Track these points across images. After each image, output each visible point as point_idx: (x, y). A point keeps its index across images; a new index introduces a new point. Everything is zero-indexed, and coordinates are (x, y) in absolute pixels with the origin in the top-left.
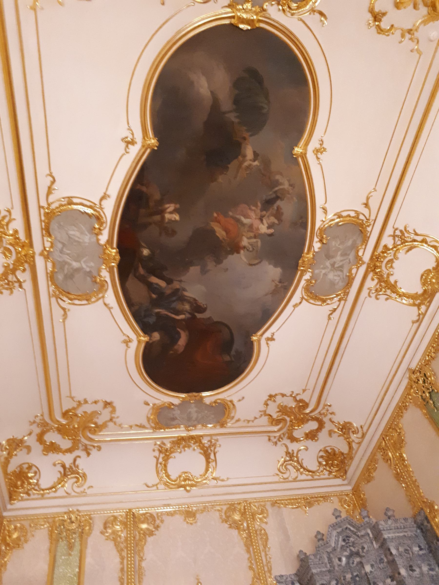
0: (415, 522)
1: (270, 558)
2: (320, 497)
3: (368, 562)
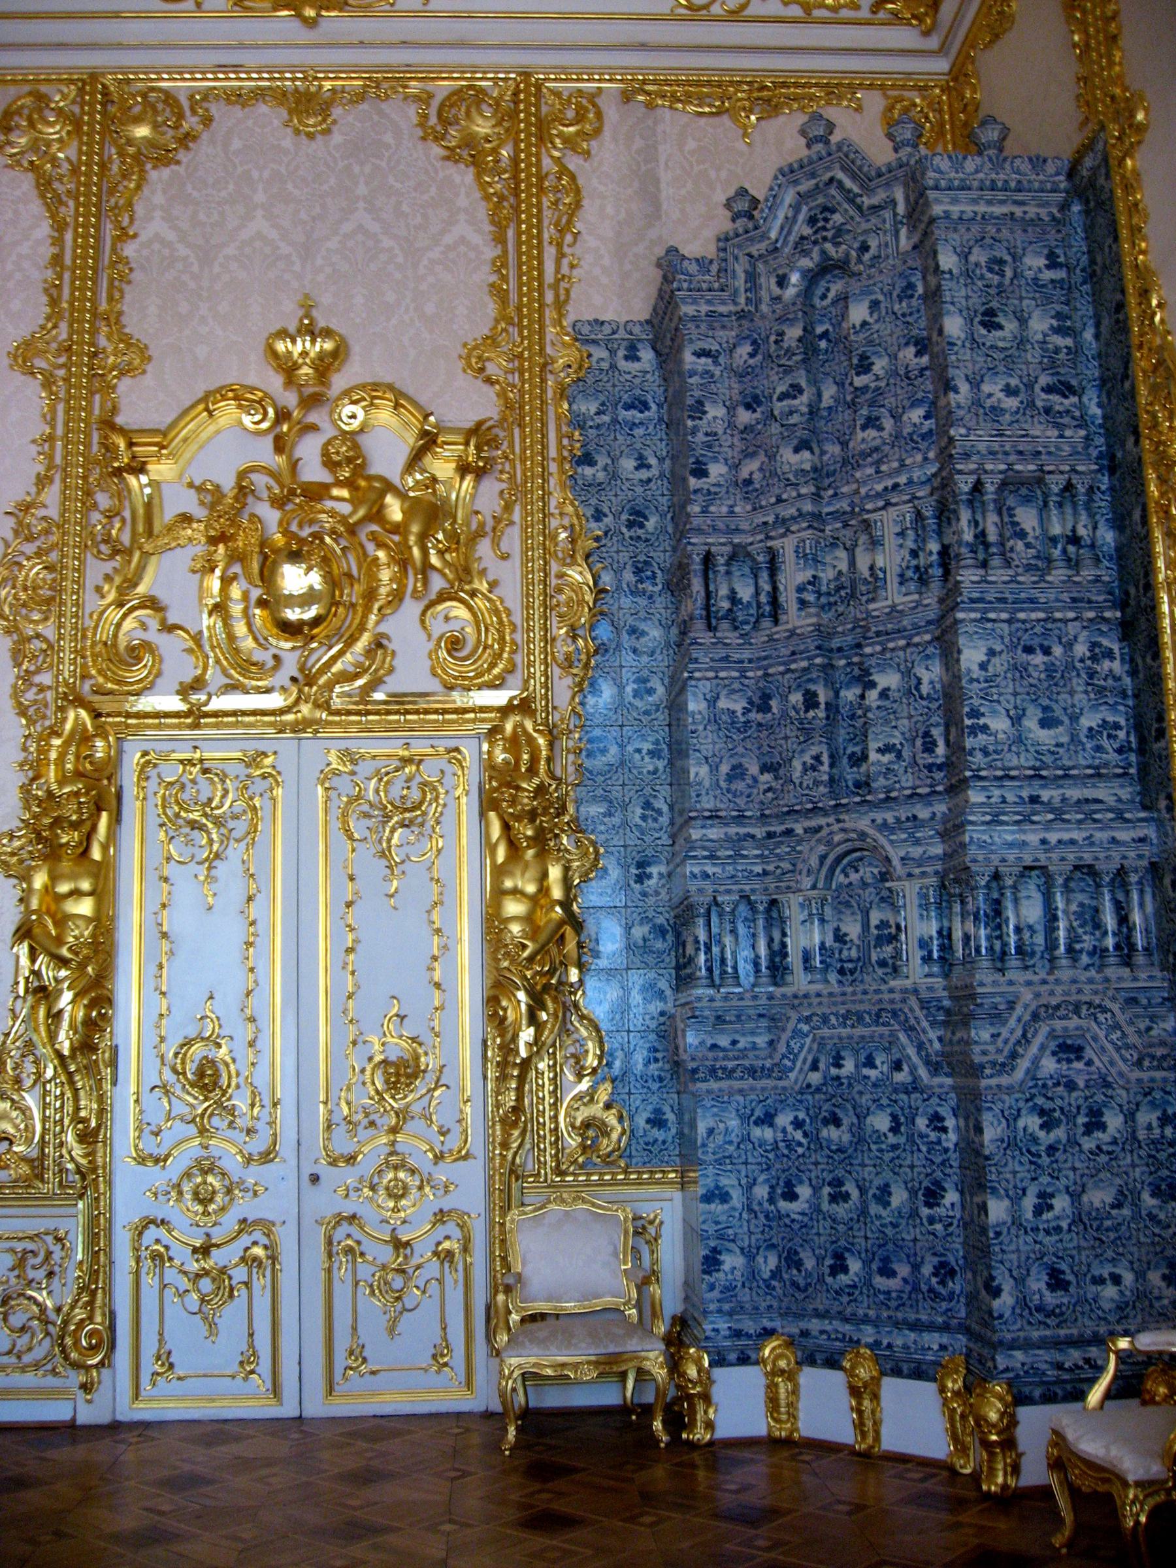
0: (1071, 175)
1: (572, 267)
2: (816, 85)
3: (865, 291)
